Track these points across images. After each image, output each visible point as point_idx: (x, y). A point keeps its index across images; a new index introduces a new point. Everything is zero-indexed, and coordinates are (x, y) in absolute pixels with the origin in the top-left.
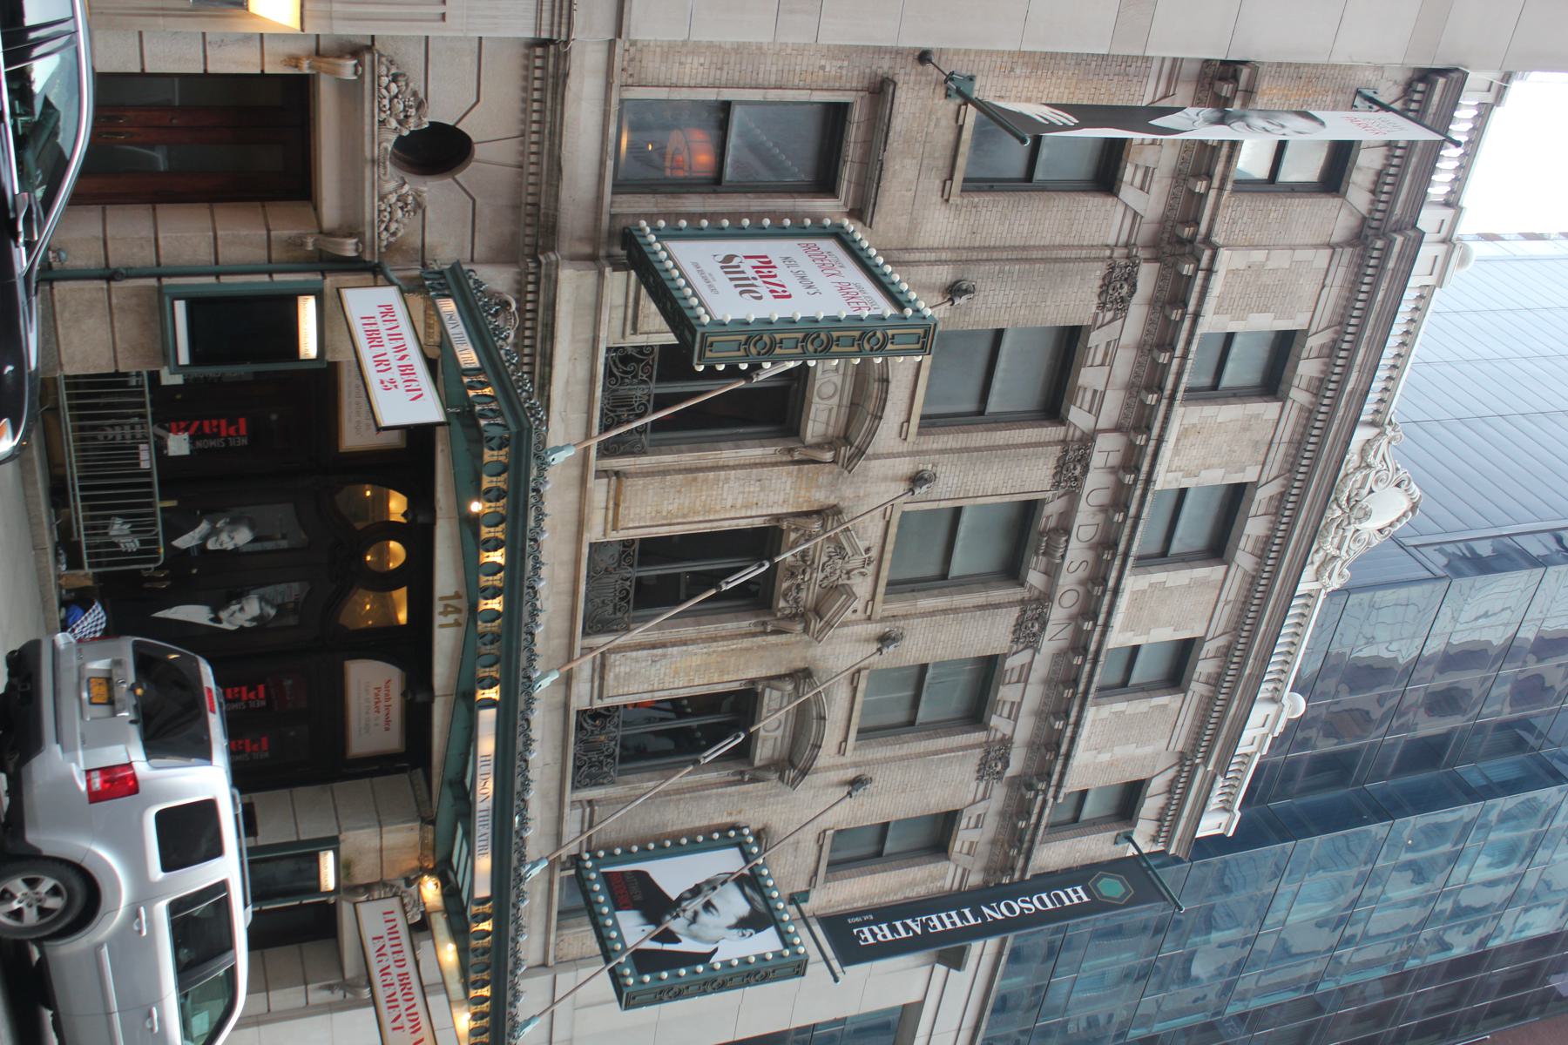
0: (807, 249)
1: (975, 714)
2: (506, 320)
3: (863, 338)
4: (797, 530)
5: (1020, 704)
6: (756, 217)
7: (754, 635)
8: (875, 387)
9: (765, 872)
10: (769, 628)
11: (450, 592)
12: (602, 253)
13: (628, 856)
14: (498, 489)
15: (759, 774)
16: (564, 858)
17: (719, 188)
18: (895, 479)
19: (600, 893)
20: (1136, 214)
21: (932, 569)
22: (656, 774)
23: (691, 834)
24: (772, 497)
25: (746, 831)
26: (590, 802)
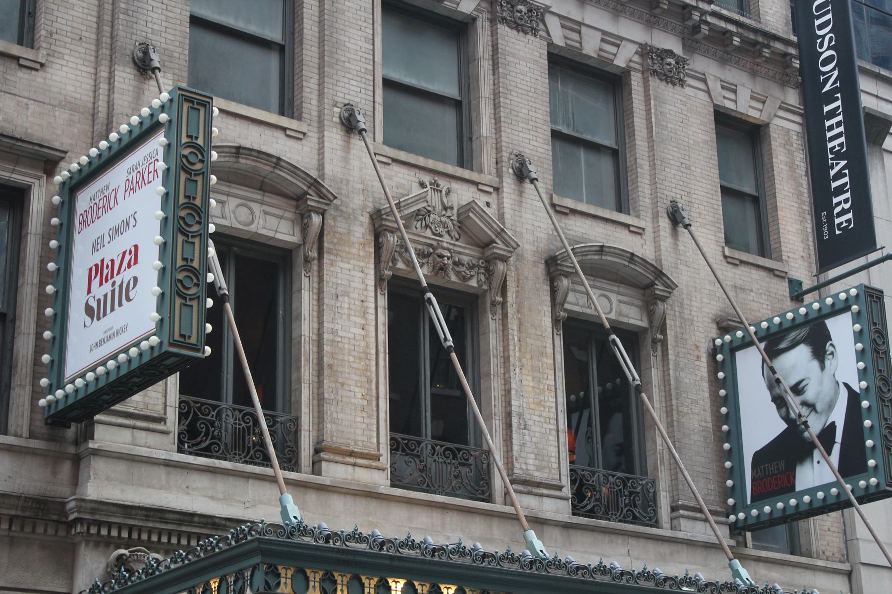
0: (85, 223)
1: (610, 82)
2: (138, 561)
3: (189, 170)
4: (394, 260)
5: (604, 33)
6: (45, 277)
7: (505, 316)
8: (244, 162)
9: (764, 325)
10: (499, 299)
12: (72, 450)
13: (736, 472)
14: (322, 580)
15: (656, 323)
16: (733, 543)
17: (10, 316)
18: (347, 149)
19: (773, 506)
21: (448, 117)
22: (648, 435)
23: (717, 402)
24: (357, 284)
25: (719, 342)
26: (674, 509)
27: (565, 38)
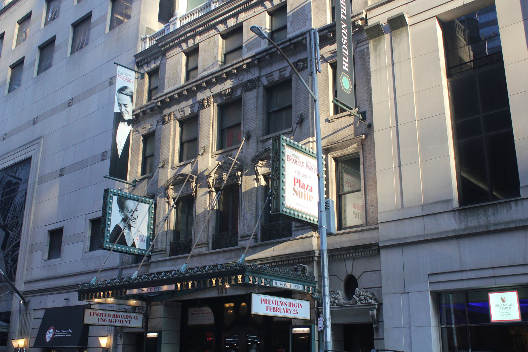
11: (217, 292)
20: (158, 123)
27: (268, 81)
